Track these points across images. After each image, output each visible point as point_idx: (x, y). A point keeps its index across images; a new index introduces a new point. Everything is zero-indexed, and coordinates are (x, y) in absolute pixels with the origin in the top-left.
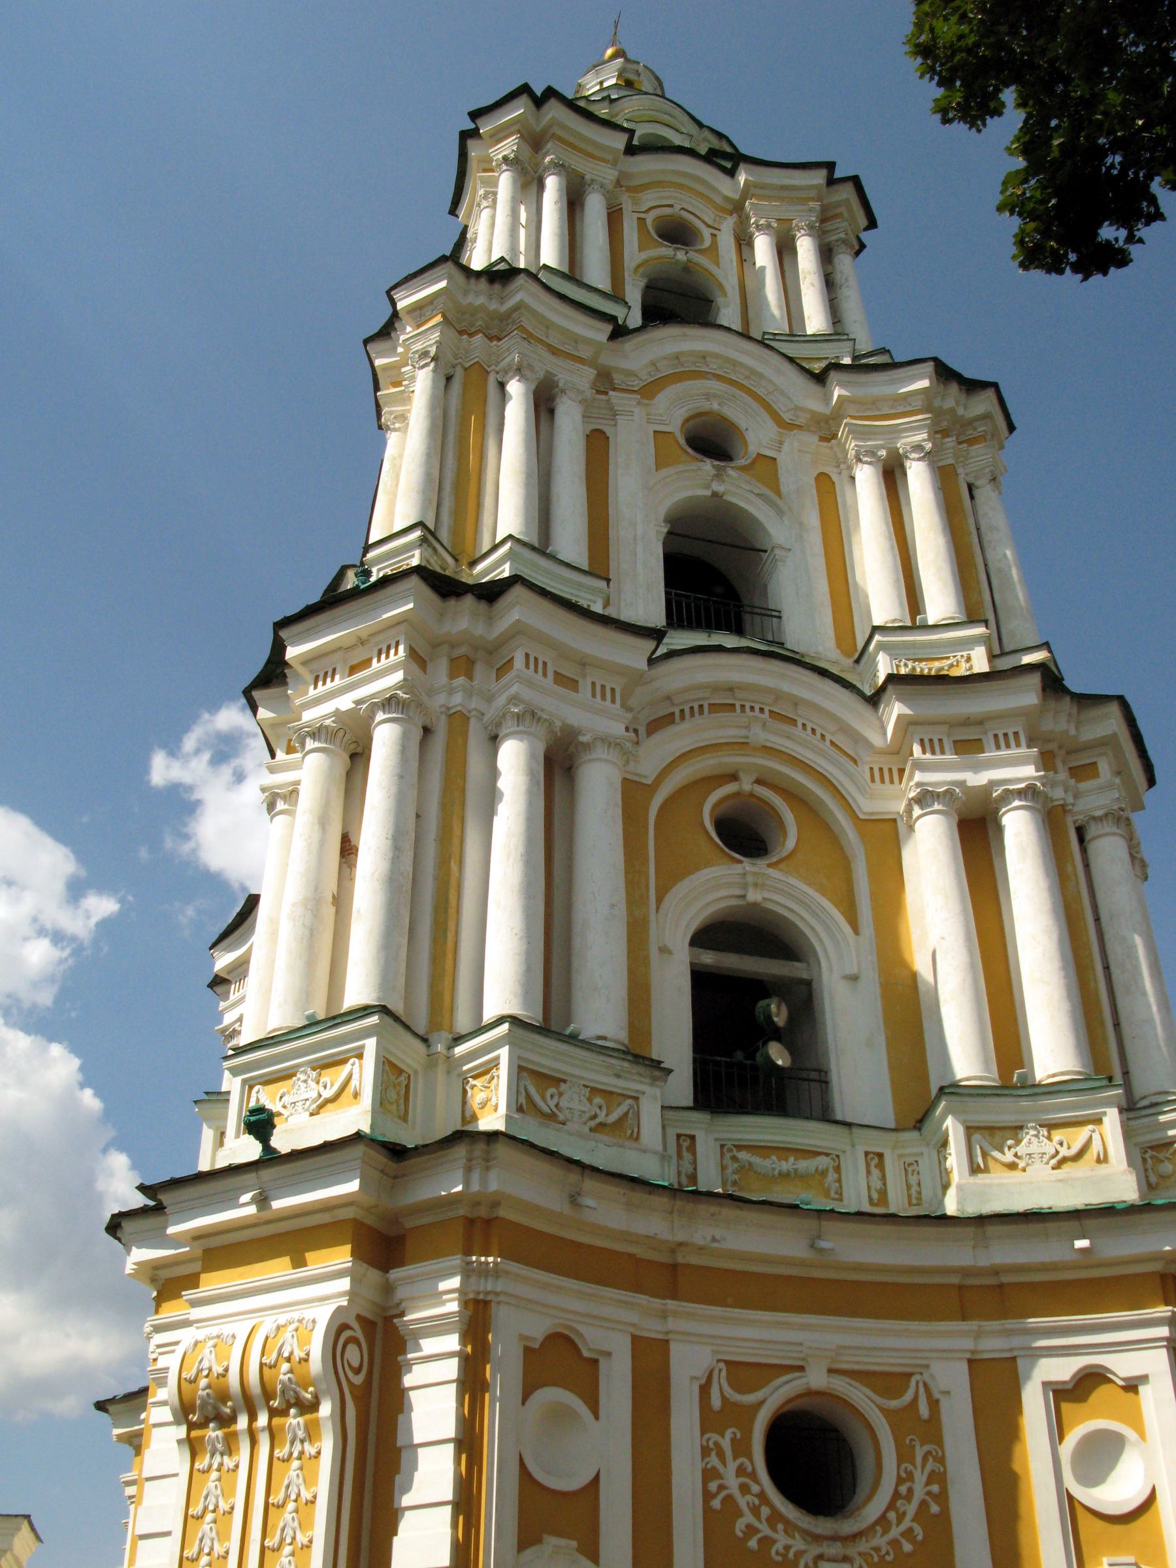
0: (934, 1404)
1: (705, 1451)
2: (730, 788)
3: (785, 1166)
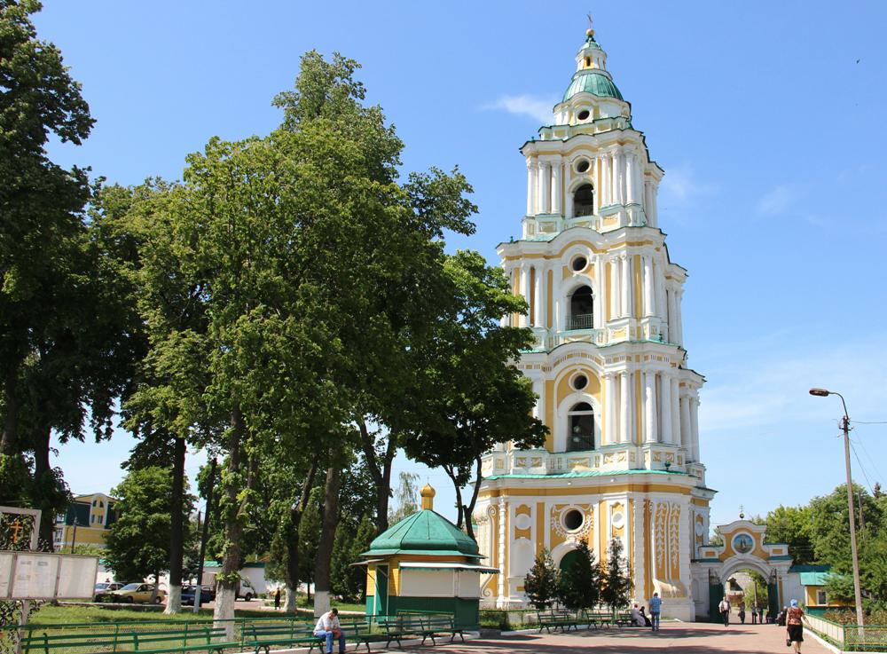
2: (576, 373)
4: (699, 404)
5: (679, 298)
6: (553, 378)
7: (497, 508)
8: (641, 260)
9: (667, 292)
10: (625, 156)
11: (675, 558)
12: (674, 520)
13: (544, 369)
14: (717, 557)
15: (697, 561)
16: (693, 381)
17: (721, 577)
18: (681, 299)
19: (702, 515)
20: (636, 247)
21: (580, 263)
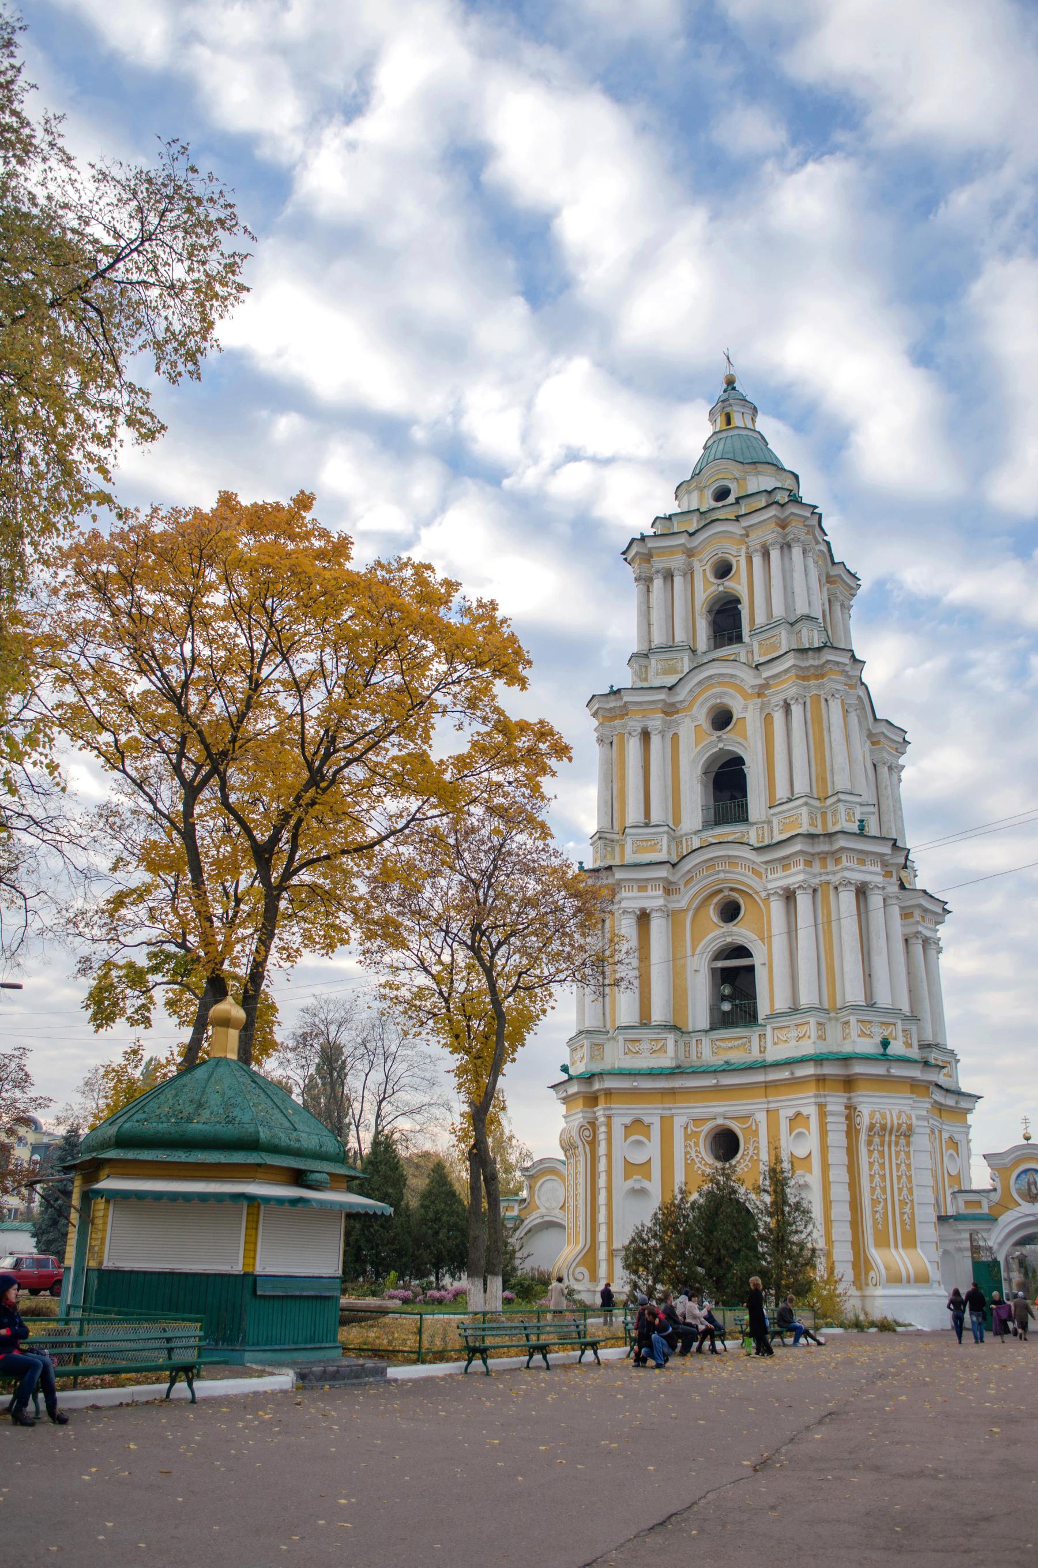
0: (757, 1125)
1: (686, 1147)
3: (730, 1045)
4: (939, 951)
5: (895, 776)
6: (683, 904)
7: (593, 1124)
8: (823, 702)
9: (875, 765)
10: (789, 546)
11: (907, 1209)
12: (902, 1141)
13: (667, 891)
14: (985, 1210)
15: (951, 1217)
16: (926, 910)
17: (995, 1247)
18: (900, 780)
19: (957, 1137)
20: (813, 682)
21: (722, 719)
